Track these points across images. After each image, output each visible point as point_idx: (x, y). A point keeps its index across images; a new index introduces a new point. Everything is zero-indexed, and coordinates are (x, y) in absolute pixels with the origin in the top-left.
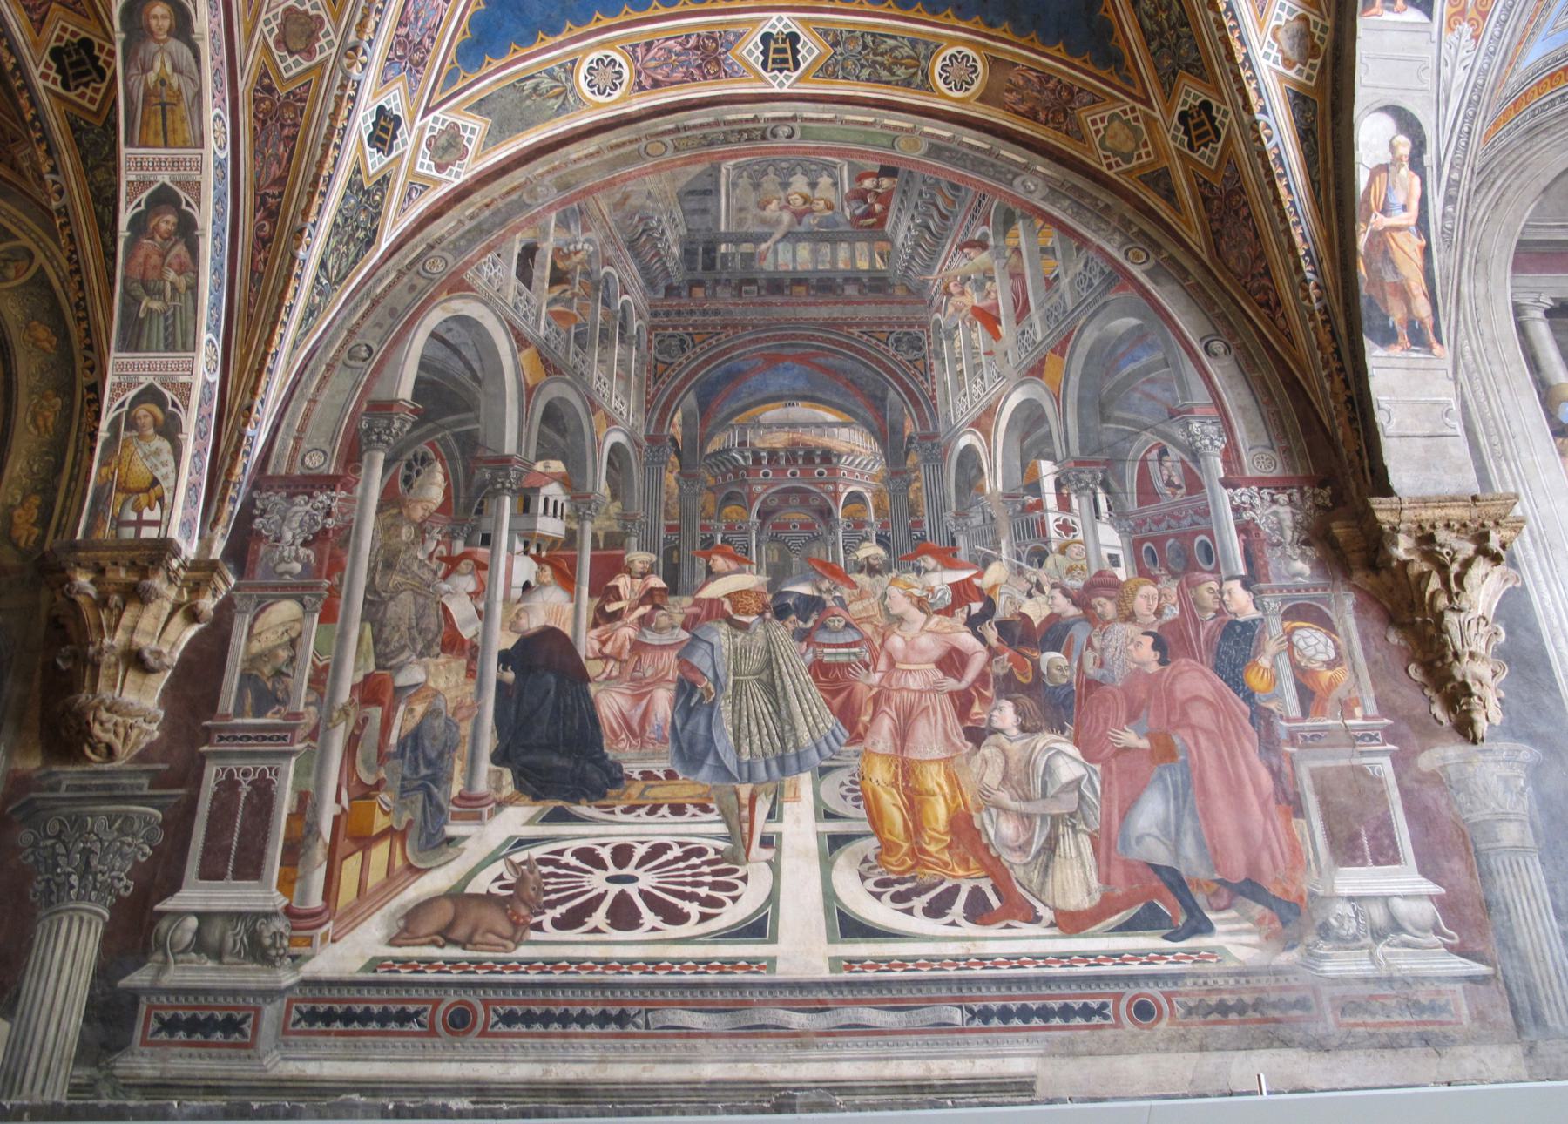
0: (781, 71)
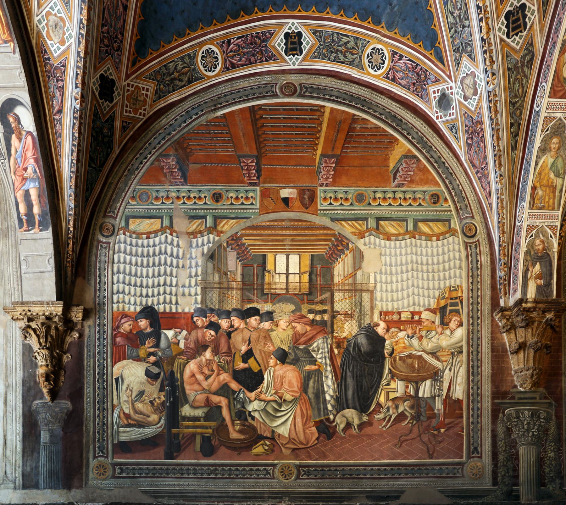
0: (294, 55)
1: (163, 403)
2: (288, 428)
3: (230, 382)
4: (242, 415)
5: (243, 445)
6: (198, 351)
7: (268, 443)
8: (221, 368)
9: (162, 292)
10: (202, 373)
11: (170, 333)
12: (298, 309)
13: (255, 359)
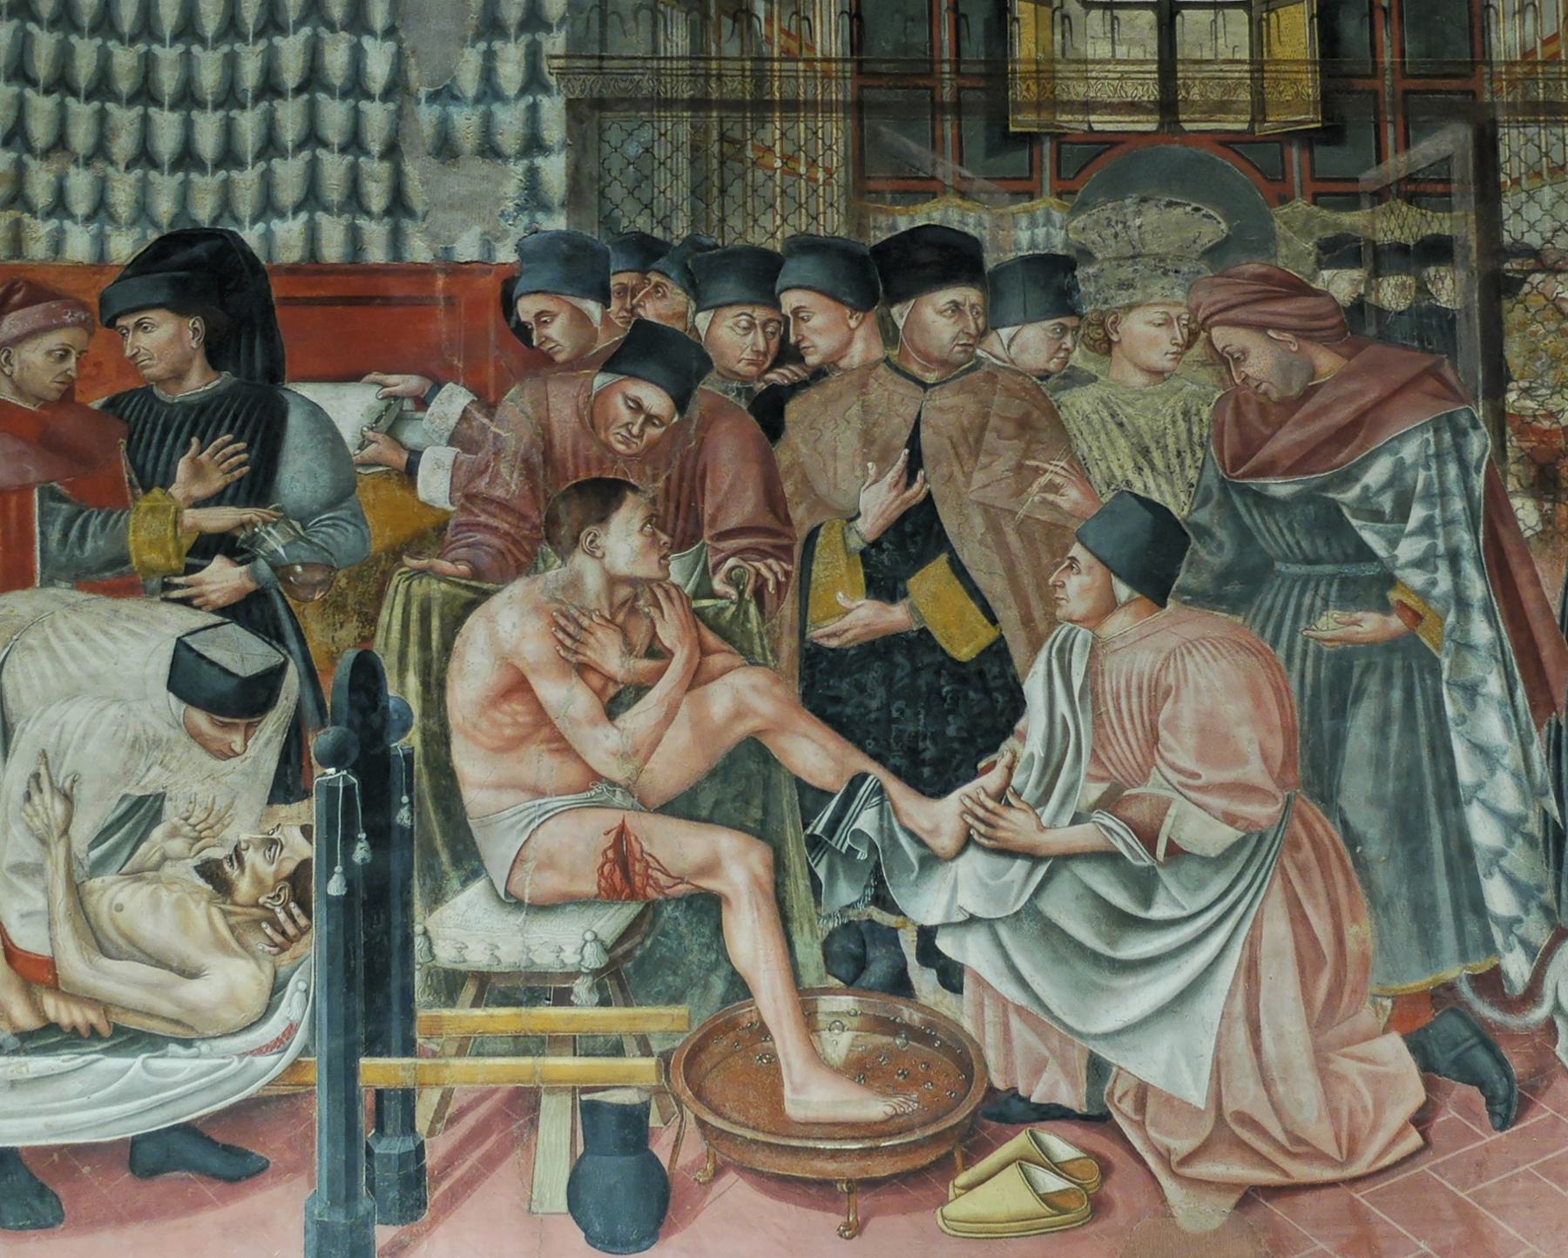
1: (298, 882)
2: (1208, 1048)
3: (779, 727)
4: (865, 956)
5: (881, 1168)
6: (552, 521)
7: (1062, 1150)
8: (718, 633)
9: (290, 132)
10: (583, 669)
11: (350, 407)
12: (1249, 236)
13: (959, 570)
